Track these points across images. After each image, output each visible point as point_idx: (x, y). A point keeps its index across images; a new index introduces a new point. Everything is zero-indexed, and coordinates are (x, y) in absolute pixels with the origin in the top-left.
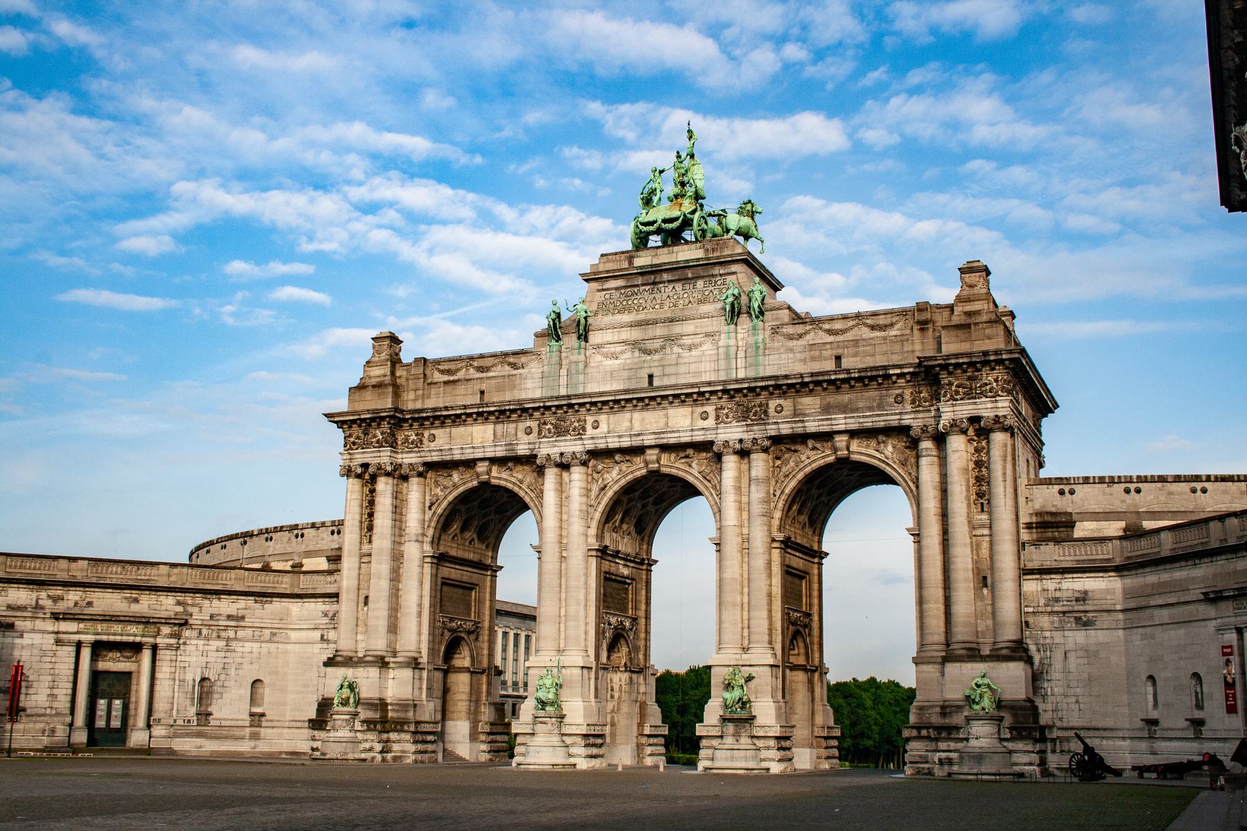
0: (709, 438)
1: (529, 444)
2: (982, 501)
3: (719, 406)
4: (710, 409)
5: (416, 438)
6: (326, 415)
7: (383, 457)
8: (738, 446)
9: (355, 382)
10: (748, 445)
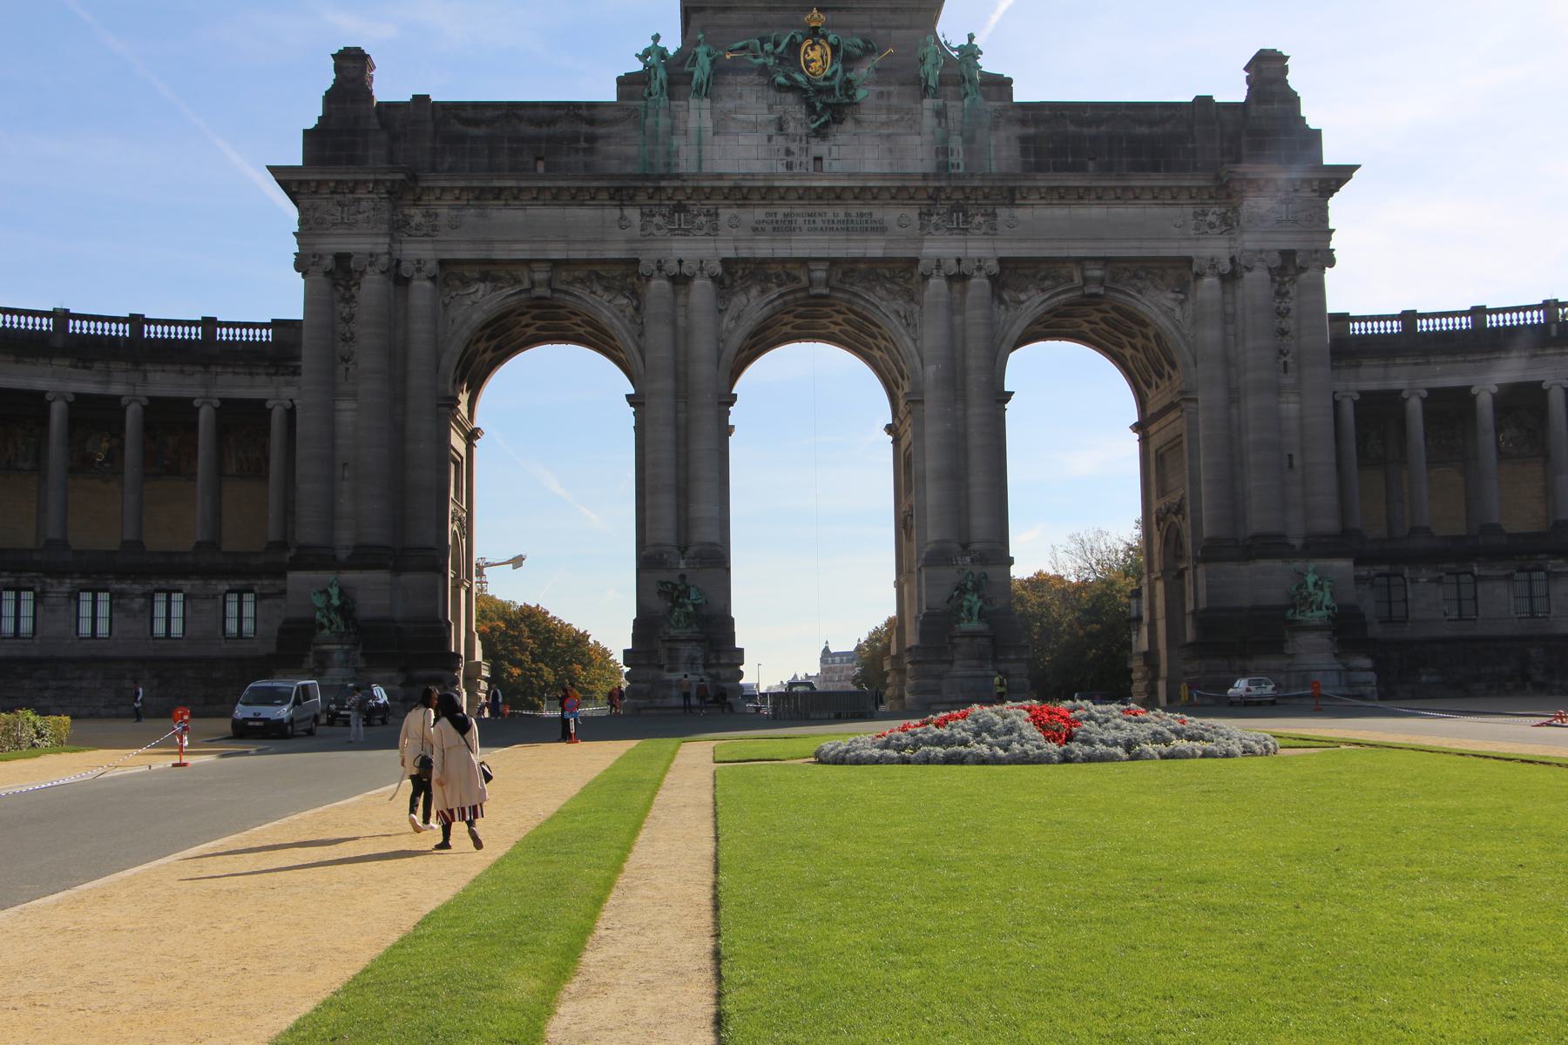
0: (910, 254)
1: (628, 241)
2: (1285, 359)
3: (925, 210)
4: (913, 213)
5: (423, 220)
6: (273, 170)
7: (380, 245)
8: (954, 270)
9: (312, 123)
10: (964, 268)
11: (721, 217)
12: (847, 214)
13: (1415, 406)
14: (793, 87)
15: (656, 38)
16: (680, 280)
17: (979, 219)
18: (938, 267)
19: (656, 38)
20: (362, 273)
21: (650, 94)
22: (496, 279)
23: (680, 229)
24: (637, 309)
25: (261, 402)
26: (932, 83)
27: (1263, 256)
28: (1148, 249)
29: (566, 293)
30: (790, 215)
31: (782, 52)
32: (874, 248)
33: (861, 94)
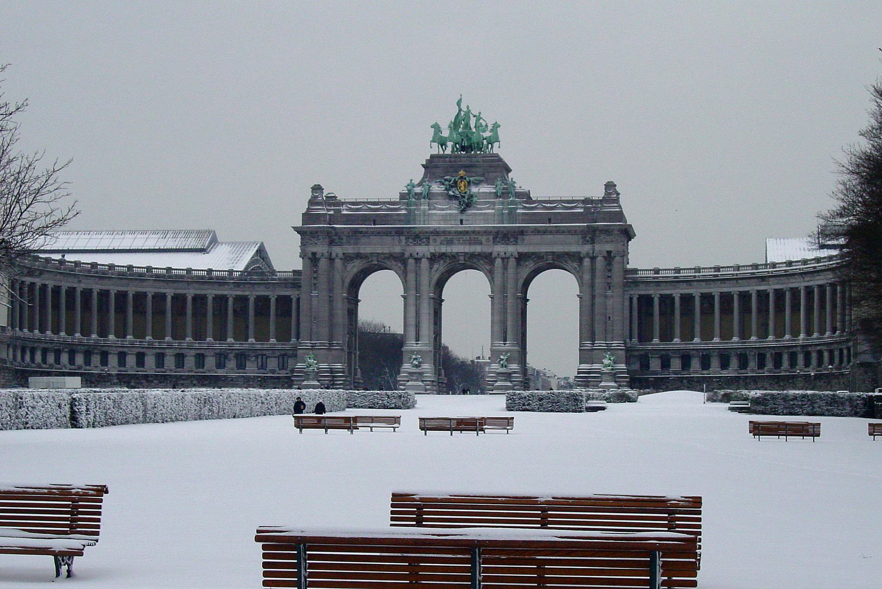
4: (491, 238)
8: (504, 256)
10: (507, 256)
11: (430, 239)
12: (470, 238)
13: (656, 301)
14: (455, 197)
15: (411, 180)
16: (418, 260)
17: (512, 240)
18: (498, 254)
19: (411, 180)
20: (319, 259)
21: (410, 198)
22: (361, 258)
23: (417, 243)
24: (405, 268)
25: (289, 297)
26: (499, 194)
27: (601, 252)
28: (566, 249)
29: (382, 262)
30: (452, 238)
31: (452, 184)
32: (478, 249)
33: (475, 199)
